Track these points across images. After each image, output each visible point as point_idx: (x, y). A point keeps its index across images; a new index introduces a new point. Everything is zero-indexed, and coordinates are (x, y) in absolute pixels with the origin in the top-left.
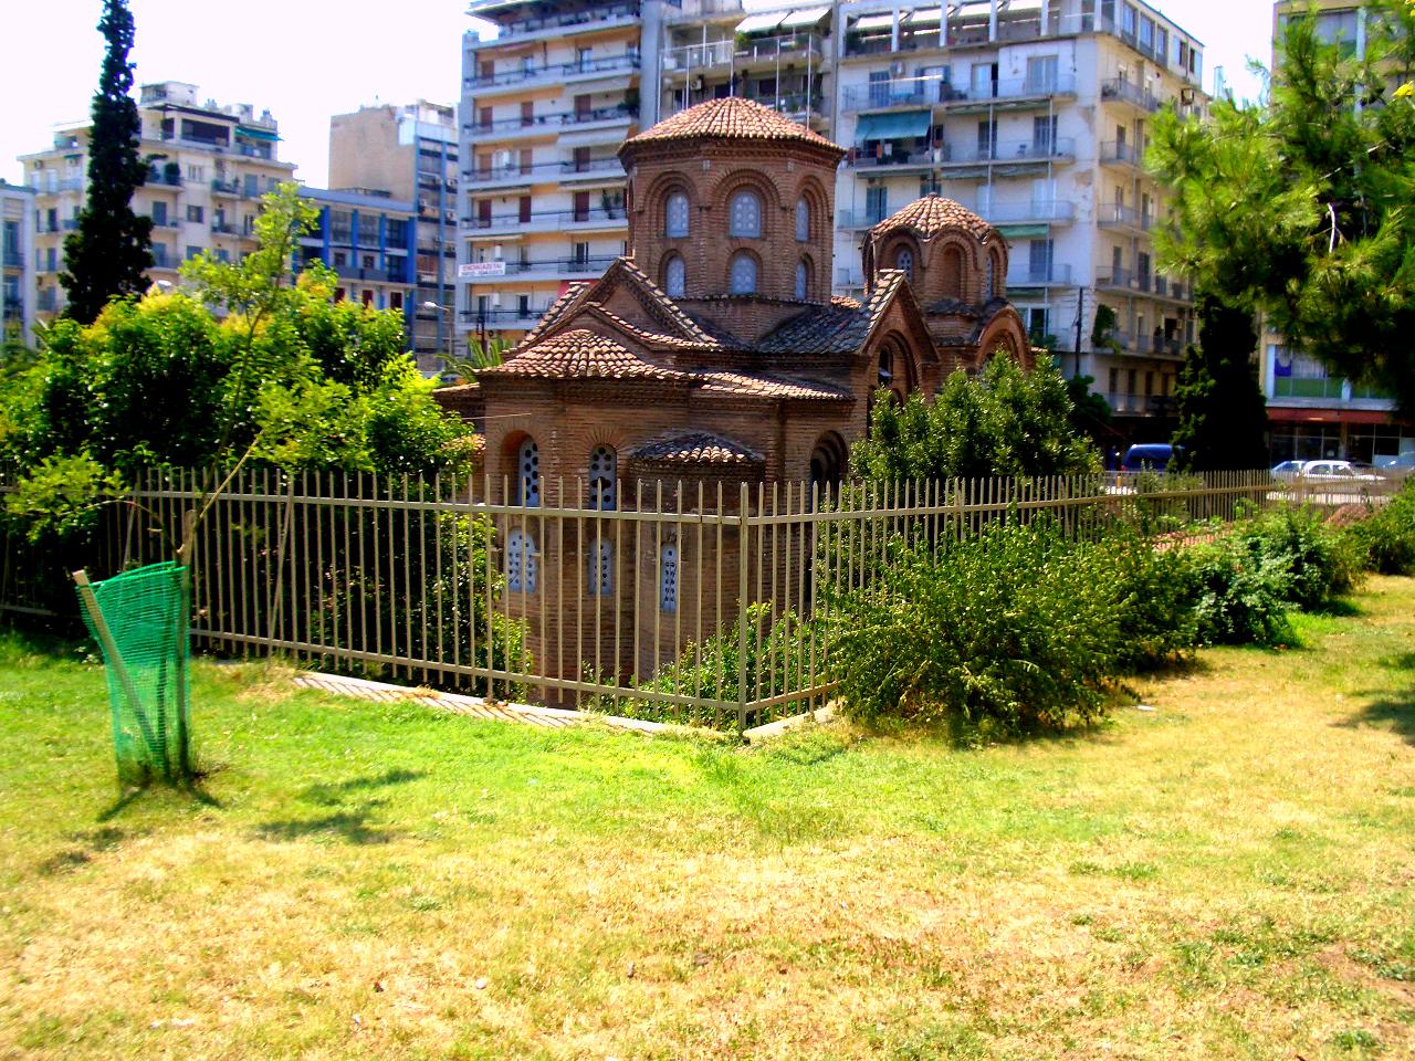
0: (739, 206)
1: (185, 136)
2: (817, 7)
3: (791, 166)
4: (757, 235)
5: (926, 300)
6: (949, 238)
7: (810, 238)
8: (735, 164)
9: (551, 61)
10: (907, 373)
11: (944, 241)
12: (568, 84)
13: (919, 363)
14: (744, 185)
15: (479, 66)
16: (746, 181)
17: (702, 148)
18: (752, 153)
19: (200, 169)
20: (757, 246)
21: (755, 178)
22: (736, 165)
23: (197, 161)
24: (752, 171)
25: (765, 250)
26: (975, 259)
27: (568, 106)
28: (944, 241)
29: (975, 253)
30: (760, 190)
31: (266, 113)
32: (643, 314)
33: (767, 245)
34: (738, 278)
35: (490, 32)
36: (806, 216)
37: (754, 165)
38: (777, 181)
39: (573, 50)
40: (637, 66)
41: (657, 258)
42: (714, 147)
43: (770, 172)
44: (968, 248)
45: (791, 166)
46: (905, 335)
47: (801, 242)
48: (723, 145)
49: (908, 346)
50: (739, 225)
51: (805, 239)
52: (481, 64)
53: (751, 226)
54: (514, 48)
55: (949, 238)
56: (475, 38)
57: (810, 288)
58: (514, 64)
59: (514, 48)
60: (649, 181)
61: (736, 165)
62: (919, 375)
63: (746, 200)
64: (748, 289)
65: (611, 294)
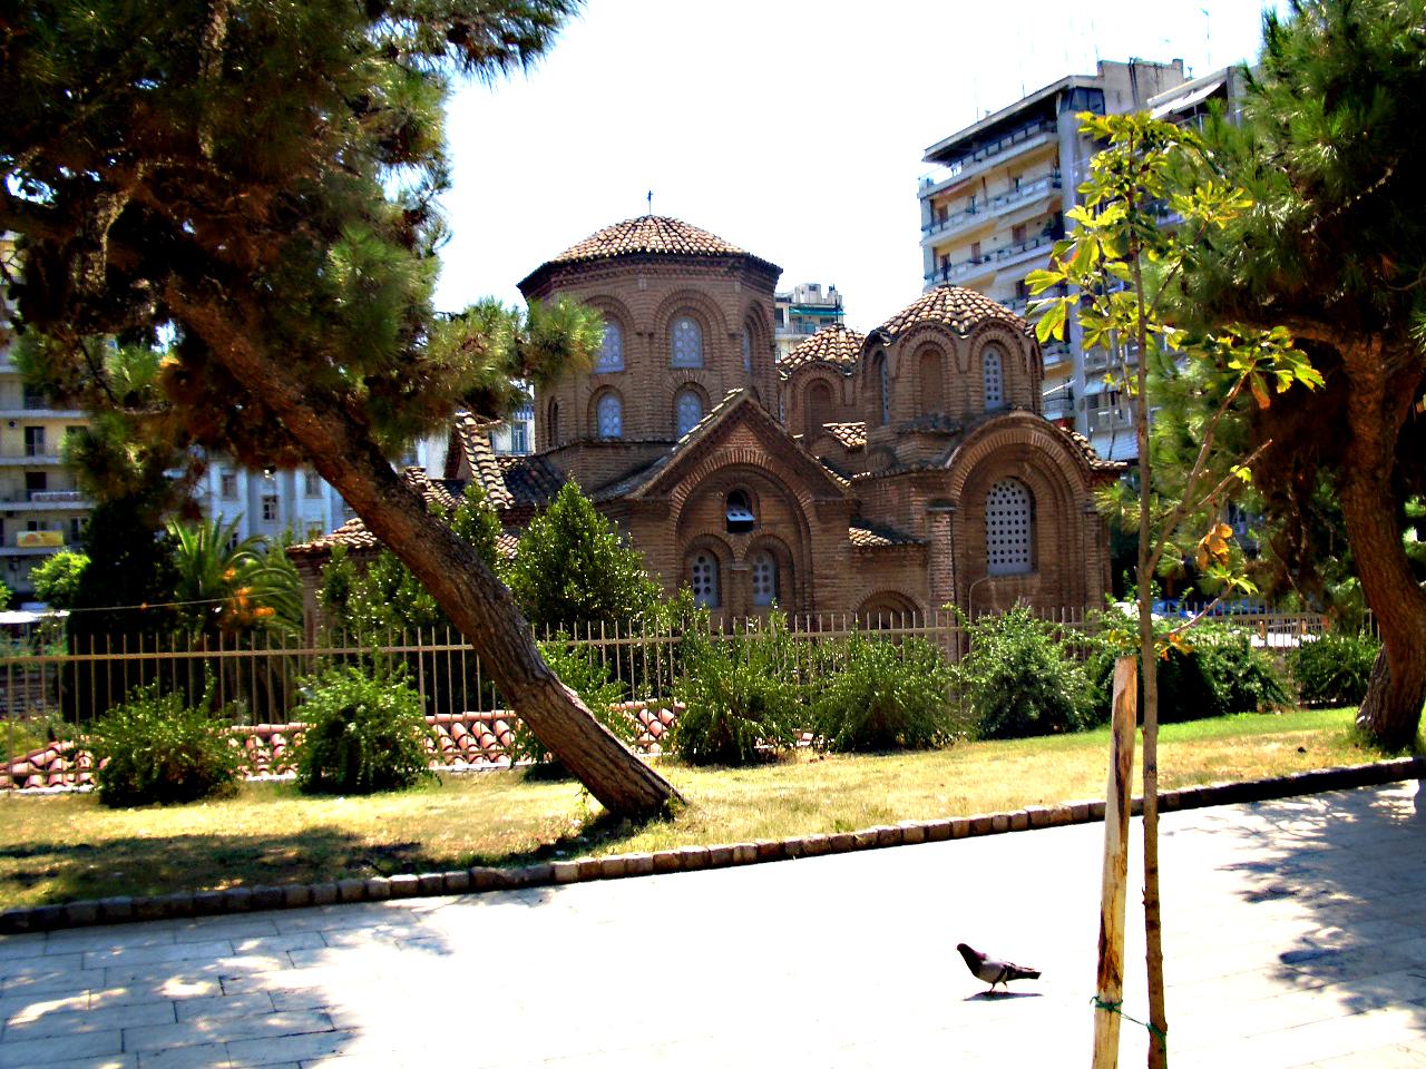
2: (1206, 85)
4: (621, 368)
5: (899, 418)
6: (921, 337)
8: (584, 291)
9: (990, 196)
10: (793, 514)
11: (915, 342)
12: (1001, 217)
13: (806, 501)
15: (937, 214)
20: (617, 382)
24: (604, 296)
25: (626, 384)
26: (957, 358)
27: (1006, 239)
28: (915, 342)
29: (956, 351)
30: (616, 317)
31: (832, 289)
33: (628, 379)
34: (607, 421)
35: (942, 174)
38: (629, 303)
39: (1007, 181)
40: (1057, 186)
43: (621, 293)
44: (948, 347)
47: (681, 369)
48: (569, 272)
50: (679, 355)
51: (700, 365)
52: (936, 206)
53: (616, 359)
54: (955, 189)
55: (921, 337)
56: (929, 183)
58: (963, 203)
59: (955, 189)
62: (812, 519)
64: (616, 432)
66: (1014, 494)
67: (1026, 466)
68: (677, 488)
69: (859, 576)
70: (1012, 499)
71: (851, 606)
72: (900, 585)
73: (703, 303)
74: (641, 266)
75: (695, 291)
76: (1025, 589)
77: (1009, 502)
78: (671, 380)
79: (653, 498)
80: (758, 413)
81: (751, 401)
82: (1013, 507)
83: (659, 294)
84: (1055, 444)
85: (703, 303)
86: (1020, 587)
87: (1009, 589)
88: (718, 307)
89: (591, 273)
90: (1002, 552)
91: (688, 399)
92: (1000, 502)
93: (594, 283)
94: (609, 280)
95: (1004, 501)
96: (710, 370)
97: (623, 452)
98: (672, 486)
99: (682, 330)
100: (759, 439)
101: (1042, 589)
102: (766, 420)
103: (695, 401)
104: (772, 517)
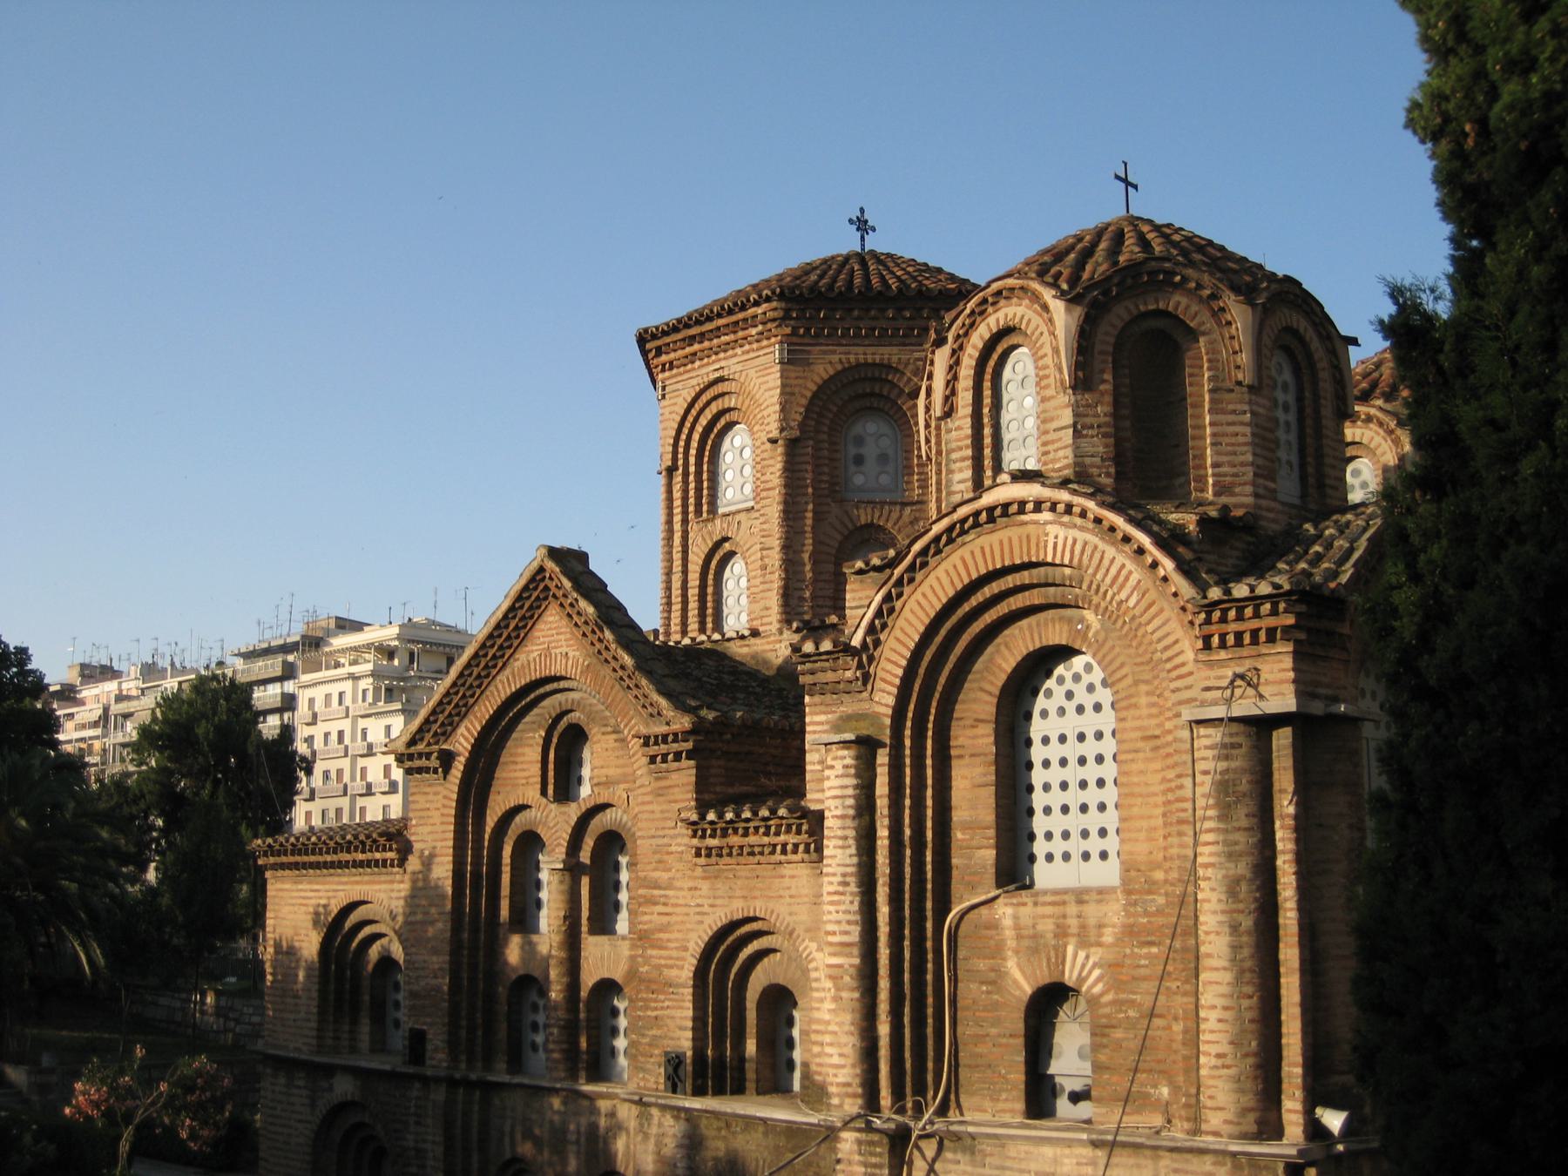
66: (1091, 688)
67: (1089, 615)
69: (705, 886)
70: (1089, 701)
71: (691, 945)
72: (771, 905)
76: (1083, 927)
77: (1080, 709)
82: (1090, 723)
84: (1110, 552)
86: (1073, 923)
87: (1047, 927)
90: (1066, 835)
92: (1062, 711)
95: (1070, 707)
101: (1130, 931)
104: (611, 772)
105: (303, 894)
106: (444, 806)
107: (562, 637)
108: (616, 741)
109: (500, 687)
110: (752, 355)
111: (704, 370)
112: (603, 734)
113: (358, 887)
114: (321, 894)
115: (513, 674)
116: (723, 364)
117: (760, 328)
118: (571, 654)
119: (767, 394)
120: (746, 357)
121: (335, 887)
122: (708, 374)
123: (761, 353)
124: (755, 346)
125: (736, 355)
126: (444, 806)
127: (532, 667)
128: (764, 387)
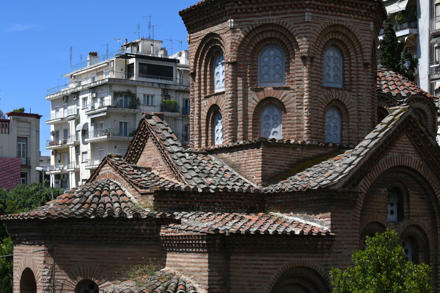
0: (266, 59)
1: (141, 72)
3: (308, 16)
7: (344, 85)
14: (268, 39)
16: (269, 35)
17: (226, 8)
18: (271, 7)
19: (152, 96)
21: (277, 32)
22: (257, 21)
23: (150, 91)
30: (282, 42)
32: (162, 163)
36: (340, 65)
37: (274, 19)
41: (204, 114)
42: (236, 6)
45: (308, 16)
46: (421, 171)
47: (329, 88)
49: (427, 182)
51: (340, 86)
57: (345, 133)
60: (197, 44)
61: (257, 21)
63: (272, 53)
65: (143, 146)
68: (361, 183)
73: (347, 37)
74: (307, 2)
75: (343, 26)
78: (323, 97)
79: (347, 189)
80: (418, 127)
81: (414, 116)
83: (319, 26)
85: (347, 37)
88: (358, 41)
89: (263, 5)
91: (331, 113)
93: (264, 13)
94: (278, 12)
96: (350, 91)
97: (291, 152)
98: (358, 181)
99: (329, 57)
100: (415, 147)
102: (422, 132)
103: (337, 115)
105: (256, 262)
106: (354, 220)
107: (410, 149)
108: (420, 198)
109: (380, 165)
110: (358, 21)
111: (337, 18)
112: (415, 194)
113: (299, 259)
114: (270, 262)
115: (386, 160)
116: (343, 19)
117: (365, 11)
118: (413, 158)
119: (365, 42)
120: (355, 21)
121: (281, 259)
122: (335, 20)
123: (363, 22)
124: (360, 17)
125: (350, 17)
126: (354, 220)
127: (395, 160)
128: (363, 38)
